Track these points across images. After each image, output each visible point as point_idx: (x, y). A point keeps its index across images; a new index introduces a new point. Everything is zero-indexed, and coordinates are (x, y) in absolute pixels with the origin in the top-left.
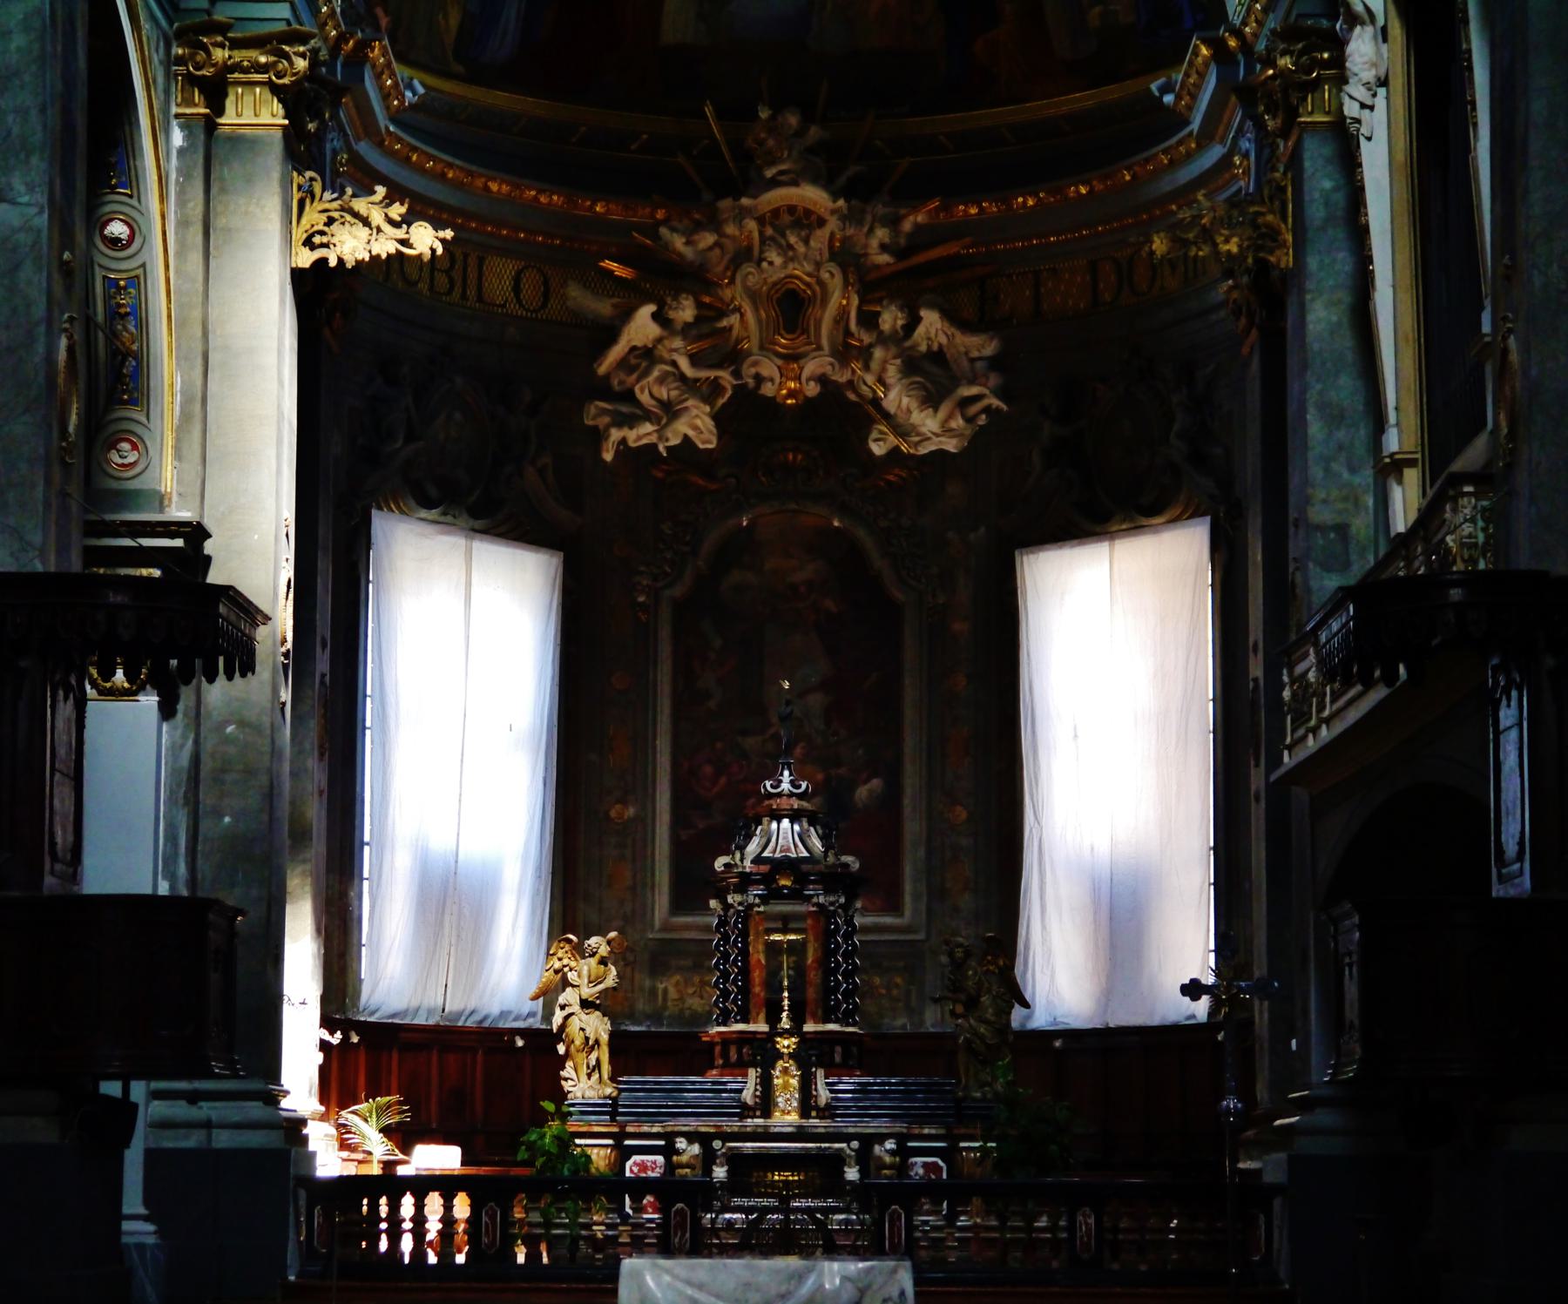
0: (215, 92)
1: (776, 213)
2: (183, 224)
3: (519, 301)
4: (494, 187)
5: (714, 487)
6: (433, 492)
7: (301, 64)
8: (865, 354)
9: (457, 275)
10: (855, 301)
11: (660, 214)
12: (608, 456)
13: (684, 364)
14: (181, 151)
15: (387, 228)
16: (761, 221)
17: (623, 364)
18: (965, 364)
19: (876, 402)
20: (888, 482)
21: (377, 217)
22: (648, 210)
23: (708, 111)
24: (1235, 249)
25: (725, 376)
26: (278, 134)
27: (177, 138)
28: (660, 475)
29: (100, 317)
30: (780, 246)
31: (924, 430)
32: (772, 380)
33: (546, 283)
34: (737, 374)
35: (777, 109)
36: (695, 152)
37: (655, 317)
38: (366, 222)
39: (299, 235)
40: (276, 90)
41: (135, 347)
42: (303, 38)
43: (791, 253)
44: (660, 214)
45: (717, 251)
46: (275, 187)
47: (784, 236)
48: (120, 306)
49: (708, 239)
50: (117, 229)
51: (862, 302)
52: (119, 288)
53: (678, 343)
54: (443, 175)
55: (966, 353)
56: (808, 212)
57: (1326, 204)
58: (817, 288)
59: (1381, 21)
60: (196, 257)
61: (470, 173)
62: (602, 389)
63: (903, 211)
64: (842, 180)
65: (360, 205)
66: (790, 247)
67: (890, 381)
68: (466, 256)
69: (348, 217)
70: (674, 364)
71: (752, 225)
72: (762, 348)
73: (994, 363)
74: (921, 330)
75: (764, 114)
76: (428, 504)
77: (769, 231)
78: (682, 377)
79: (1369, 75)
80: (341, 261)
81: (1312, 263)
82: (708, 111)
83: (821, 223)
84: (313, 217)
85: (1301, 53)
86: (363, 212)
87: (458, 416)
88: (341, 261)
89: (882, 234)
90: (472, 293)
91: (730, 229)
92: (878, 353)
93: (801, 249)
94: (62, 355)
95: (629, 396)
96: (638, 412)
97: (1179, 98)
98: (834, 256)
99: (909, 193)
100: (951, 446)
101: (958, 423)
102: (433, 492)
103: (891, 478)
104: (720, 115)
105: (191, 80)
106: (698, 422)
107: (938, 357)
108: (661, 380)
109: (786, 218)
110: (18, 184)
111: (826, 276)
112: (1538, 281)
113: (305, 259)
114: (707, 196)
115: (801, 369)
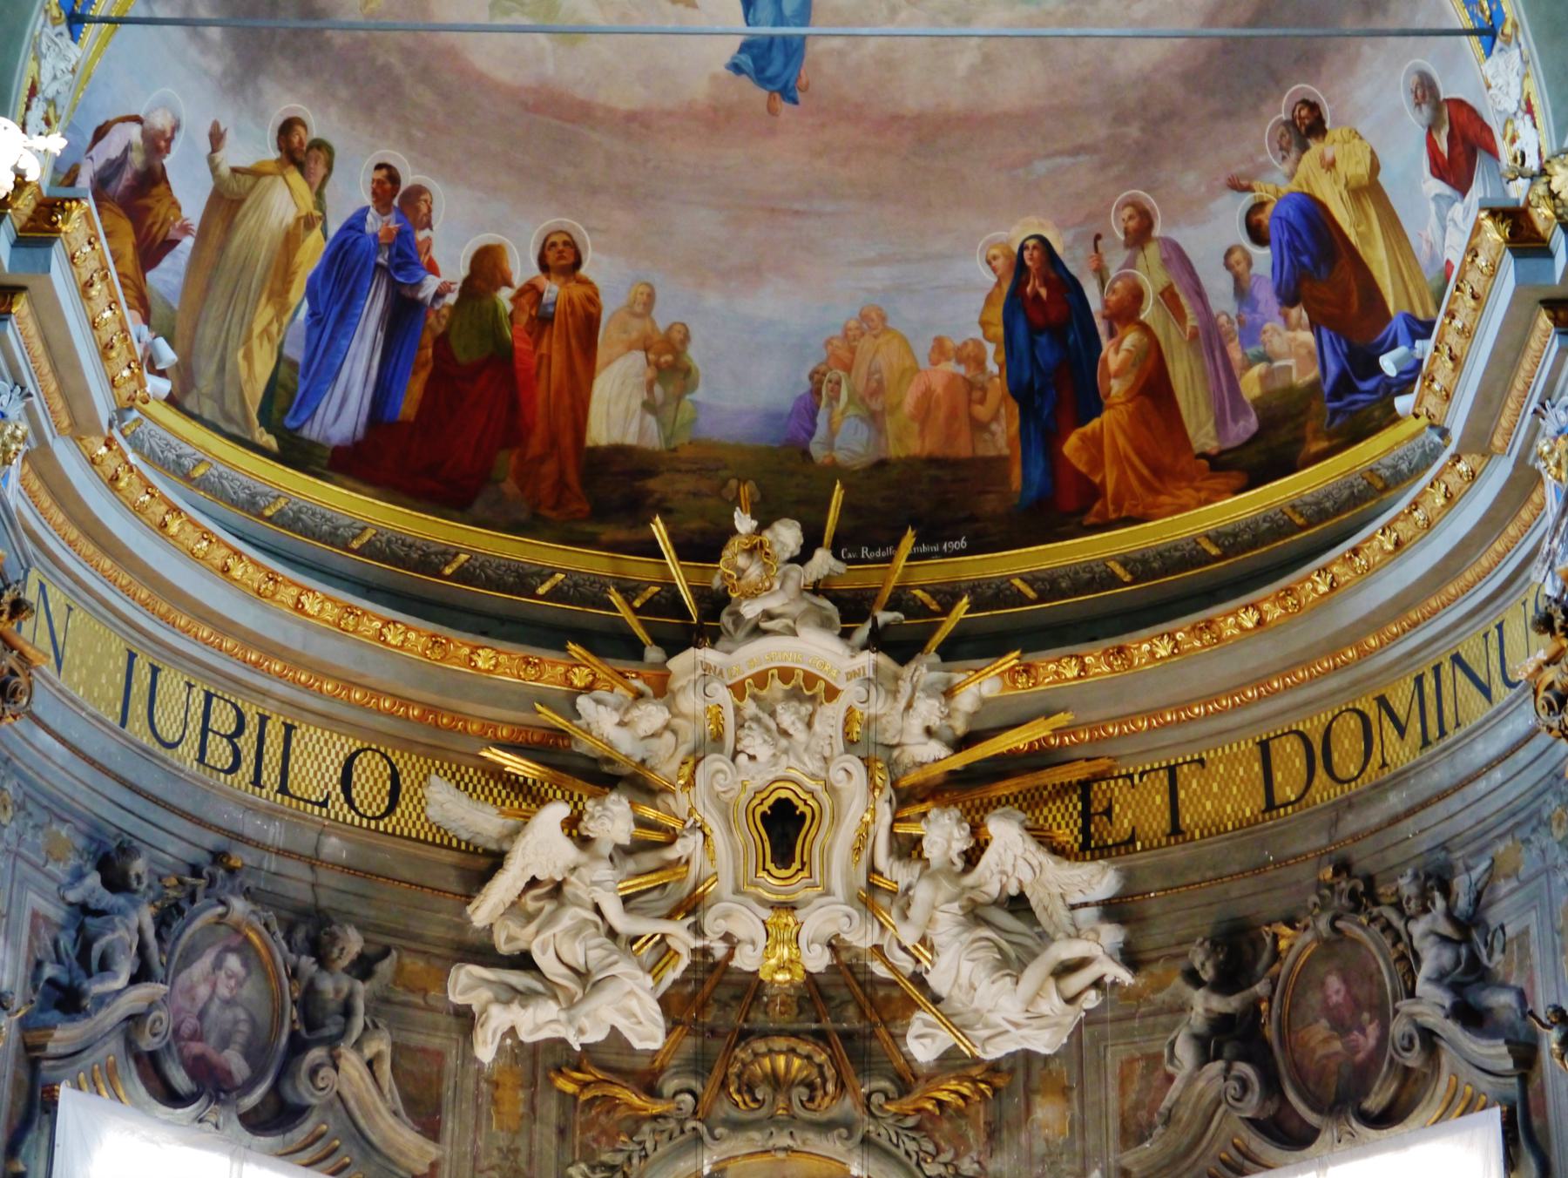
1: (761, 679)
3: (349, 800)
4: (311, 605)
5: (658, 1108)
6: (181, 1080)
8: (903, 899)
9: (247, 743)
10: (885, 815)
12: (485, 1052)
13: (613, 909)
16: (738, 690)
17: (514, 908)
18: (1063, 915)
19: (919, 980)
20: (940, 1104)
22: (561, 669)
23: (659, 529)
25: (679, 934)
28: (570, 1088)
30: (768, 730)
31: (996, 1018)
32: (753, 943)
33: (395, 777)
34: (697, 930)
36: (637, 604)
37: (571, 825)
43: (784, 742)
44: (580, 677)
45: (668, 736)
47: (773, 714)
49: (652, 715)
51: (896, 820)
53: (603, 871)
54: (225, 570)
55: (1062, 896)
56: (810, 679)
58: (824, 797)
61: (272, 577)
62: (483, 953)
63: (958, 678)
66: (785, 733)
67: (937, 940)
68: (263, 720)
70: (597, 909)
71: (724, 697)
72: (737, 891)
73: (1112, 910)
74: (988, 859)
75: (744, 523)
76: (173, 1098)
77: (750, 708)
78: (612, 934)
82: (659, 529)
83: (832, 693)
87: (233, 962)
89: (928, 710)
90: (271, 776)
91: (690, 702)
92: (922, 893)
93: (799, 733)
95: (524, 961)
96: (539, 987)
98: (850, 744)
100: (1044, 1042)
101: (1052, 1004)
102: (181, 1080)
103: (944, 1096)
106: (633, 1004)
107: (1018, 904)
108: (576, 931)
109: (777, 687)
111: (837, 776)
114: (653, 654)
115: (799, 924)
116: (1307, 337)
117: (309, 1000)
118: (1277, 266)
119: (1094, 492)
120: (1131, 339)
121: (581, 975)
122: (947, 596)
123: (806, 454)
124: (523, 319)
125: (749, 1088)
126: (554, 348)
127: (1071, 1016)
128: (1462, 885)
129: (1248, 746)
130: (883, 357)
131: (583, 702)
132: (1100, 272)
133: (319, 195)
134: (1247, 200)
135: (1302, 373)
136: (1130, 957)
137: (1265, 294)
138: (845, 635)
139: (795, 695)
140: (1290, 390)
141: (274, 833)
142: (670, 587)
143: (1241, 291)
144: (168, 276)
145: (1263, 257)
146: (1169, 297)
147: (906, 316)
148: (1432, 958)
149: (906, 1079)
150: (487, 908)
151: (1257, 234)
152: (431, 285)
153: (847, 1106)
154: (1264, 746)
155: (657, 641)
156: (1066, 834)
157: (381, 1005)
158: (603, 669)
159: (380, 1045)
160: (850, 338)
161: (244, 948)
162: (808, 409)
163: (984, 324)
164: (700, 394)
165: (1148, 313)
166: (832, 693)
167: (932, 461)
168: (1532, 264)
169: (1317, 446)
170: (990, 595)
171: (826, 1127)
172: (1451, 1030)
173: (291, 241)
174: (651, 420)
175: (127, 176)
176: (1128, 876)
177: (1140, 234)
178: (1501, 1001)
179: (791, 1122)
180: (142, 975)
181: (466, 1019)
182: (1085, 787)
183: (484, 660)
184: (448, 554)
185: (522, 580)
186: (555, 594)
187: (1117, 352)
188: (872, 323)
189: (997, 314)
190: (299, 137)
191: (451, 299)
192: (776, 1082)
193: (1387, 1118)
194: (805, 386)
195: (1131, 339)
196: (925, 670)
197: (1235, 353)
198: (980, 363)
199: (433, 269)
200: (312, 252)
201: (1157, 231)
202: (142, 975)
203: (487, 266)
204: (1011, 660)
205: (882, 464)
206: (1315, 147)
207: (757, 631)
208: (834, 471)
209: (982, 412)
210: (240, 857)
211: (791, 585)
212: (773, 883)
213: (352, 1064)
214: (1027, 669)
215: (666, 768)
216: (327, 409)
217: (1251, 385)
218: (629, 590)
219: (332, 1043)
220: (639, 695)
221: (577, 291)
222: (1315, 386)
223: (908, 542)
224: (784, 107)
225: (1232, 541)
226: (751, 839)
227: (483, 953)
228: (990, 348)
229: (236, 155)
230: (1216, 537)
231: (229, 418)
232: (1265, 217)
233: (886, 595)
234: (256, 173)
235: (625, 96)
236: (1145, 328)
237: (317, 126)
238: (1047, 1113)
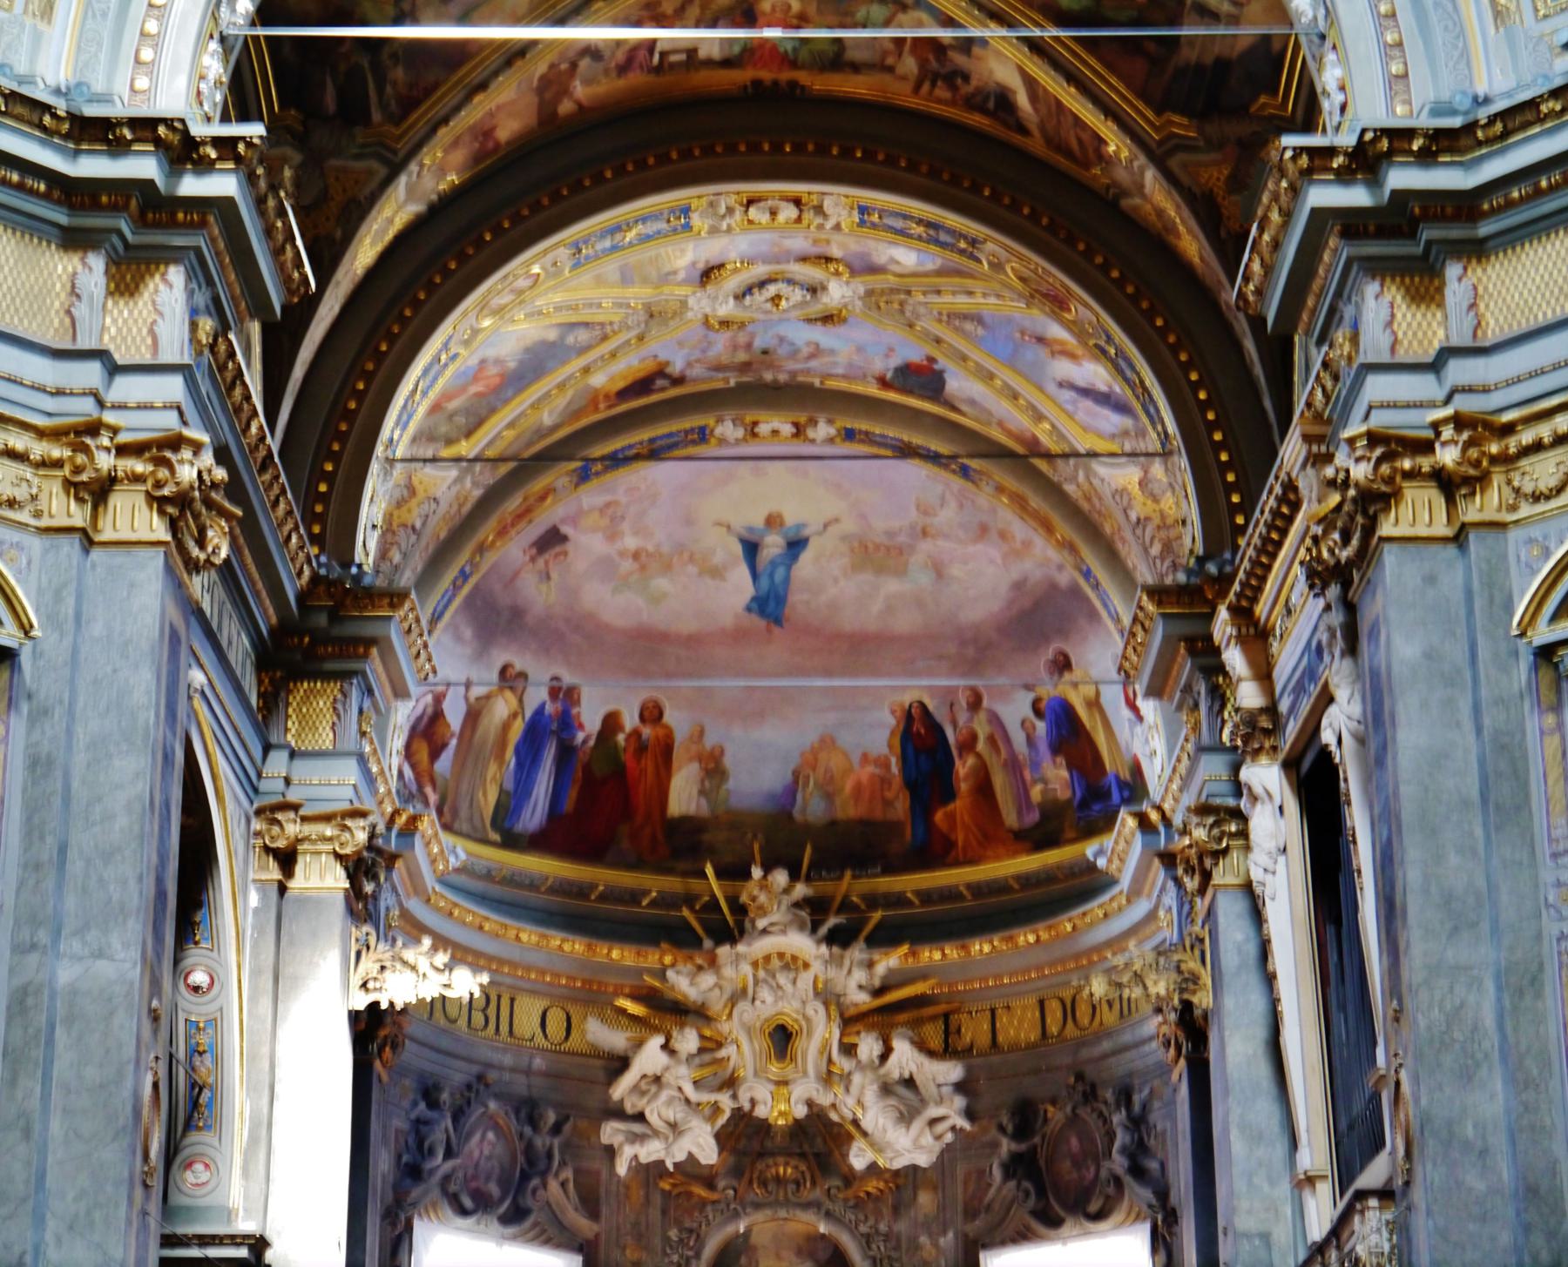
0: (287, 859)
1: (767, 958)
2: (256, 973)
3: (546, 1036)
4: (524, 937)
5: (714, 1196)
6: (468, 1202)
7: (362, 837)
8: (846, 1079)
9: (492, 1011)
10: (836, 1033)
11: (668, 959)
12: (622, 1169)
13: (689, 1089)
14: (256, 911)
15: (431, 973)
16: (755, 965)
17: (636, 1089)
18: (934, 1090)
19: (856, 1122)
20: (868, 1194)
21: (423, 964)
22: (657, 957)
23: (709, 870)
24: (1163, 992)
25: (725, 1101)
26: (341, 895)
27: (254, 899)
28: (667, 1187)
29: (181, 1054)
30: (771, 987)
31: (898, 1147)
32: (765, 1104)
33: (568, 1014)
34: (735, 1097)
35: (767, 869)
36: (697, 907)
37: (666, 1047)
38: (414, 968)
39: (356, 981)
40: (338, 856)
41: (211, 1080)
42: (363, 814)
43: (780, 993)
45: (717, 991)
46: (337, 939)
47: (774, 977)
48: (198, 1044)
49: (707, 980)
50: (199, 978)
51: (842, 1035)
52: (198, 1029)
53: (683, 1070)
55: (934, 1080)
56: (794, 958)
57: (1240, 951)
58: (804, 1023)
59: (1277, 802)
60: (266, 1003)
62: (618, 1113)
63: (876, 957)
64: (823, 930)
65: (409, 955)
66: (779, 987)
67: (866, 1104)
68: (499, 997)
69: (398, 966)
70: (680, 1089)
71: (746, 969)
72: (756, 1074)
73: (960, 1087)
74: (893, 1059)
75: (757, 872)
76: (463, 1212)
77: (761, 974)
78: (688, 1101)
79: (1271, 845)
80: (392, 1004)
81: (1229, 1002)
82: (709, 870)
83: (806, 966)
84: (368, 965)
85: (1212, 826)
86: (411, 960)
87: (491, 1135)
88: (392, 1004)
89: (859, 976)
90: (504, 1028)
91: (728, 972)
92: (857, 1079)
93: (789, 988)
94: (147, 1090)
95: (640, 1117)
96: (649, 1132)
97: (1110, 861)
98: (817, 994)
99: (884, 938)
100: (923, 1160)
101: (927, 1139)
102: (468, 1202)
103: (870, 1189)
104: (719, 875)
105: (267, 850)
106: (701, 1140)
107: (910, 1083)
108: (670, 1102)
109: (776, 963)
110: (116, 942)
111: (810, 1012)
112: (1422, 1022)
113: (361, 1002)
114: (708, 944)
115: (790, 1094)
116: (1065, 773)
117: (529, 1149)
118: (1049, 732)
119: (949, 844)
120: (971, 761)
121: (673, 1126)
122: (873, 901)
123: (790, 816)
124: (631, 749)
125: (764, 1184)
126: (649, 764)
127: (937, 1147)
128: (1137, 1099)
129: (1032, 1001)
130: (835, 762)
131: (670, 974)
132: (954, 723)
133: (521, 701)
134: (1031, 696)
135: (1063, 794)
136: (970, 1114)
137: (1043, 747)
138: (814, 930)
139: (786, 967)
140: (1056, 801)
141: (508, 1060)
142: (713, 896)
143: (1030, 741)
144: (444, 764)
145: (1041, 727)
146: (991, 740)
147: (846, 739)
148: (1121, 1138)
149: (850, 1178)
150: (620, 1089)
151: (1038, 712)
152: (580, 736)
153: (817, 1194)
154: (1042, 1003)
155: (710, 932)
156: (936, 1042)
157: (565, 1147)
158: (681, 954)
159: (568, 1173)
160: (815, 752)
161: (497, 1127)
162: (791, 791)
163: (890, 746)
164: (731, 784)
165: (981, 746)
166: (806, 966)
167: (865, 824)
168: (1149, 838)
169: (1070, 834)
170: (899, 900)
171: (807, 1206)
172: (1128, 1180)
173: (506, 727)
174: (703, 802)
175: (426, 719)
176: (969, 1070)
177: (975, 703)
178: (1153, 1165)
179: (787, 1203)
180: (449, 1154)
181: (611, 1152)
182: (946, 1016)
183: (615, 954)
184: (593, 886)
185: (634, 897)
186: (653, 904)
187: (963, 768)
188: (827, 742)
189: (897, 742)
190: (510, 672)
191: (592, 743)
192: (778, 1180)
193: (1099, 1216)
194: (789, 777)
195: (971, 761)
196: (857, 952)
197: (1027, 775)
198: (887, 766)
199: (581, 726)
200: (517, 729)
201: (985, 703)
202: (449, 1154)
203: (611, 723)
204: (905, 949)
205: (833, 823)
206: (1067, 676)
207: (765, 932)
208: (807, 830)
209: (889, 795)
210: (492, 1076)
211: (783, 907)
212: (774, 1069)
213: (554, 1185)
214: (914, 954)
215: (717, 1005)
216: (526, 814)
217: (1036, 793)
218: (689, 900)
219: (544, 1174)
220: (700, 968)
221: (661, 732)
222: (1069, 802)
223: (848, 874)
224: (776, 630)
225: (1027, 881)
226: (762, 1044)
227: (618, 1113)
228: (893, 760)
229: (477, 691)
230: (1018, 878)
231: (474, 828)
232: (1043, 705)
233: (839, 899)
234: (488, 697)
235: (688, 626)
236: (979, 756)
237: (519, 664)
238: (925, 1199)
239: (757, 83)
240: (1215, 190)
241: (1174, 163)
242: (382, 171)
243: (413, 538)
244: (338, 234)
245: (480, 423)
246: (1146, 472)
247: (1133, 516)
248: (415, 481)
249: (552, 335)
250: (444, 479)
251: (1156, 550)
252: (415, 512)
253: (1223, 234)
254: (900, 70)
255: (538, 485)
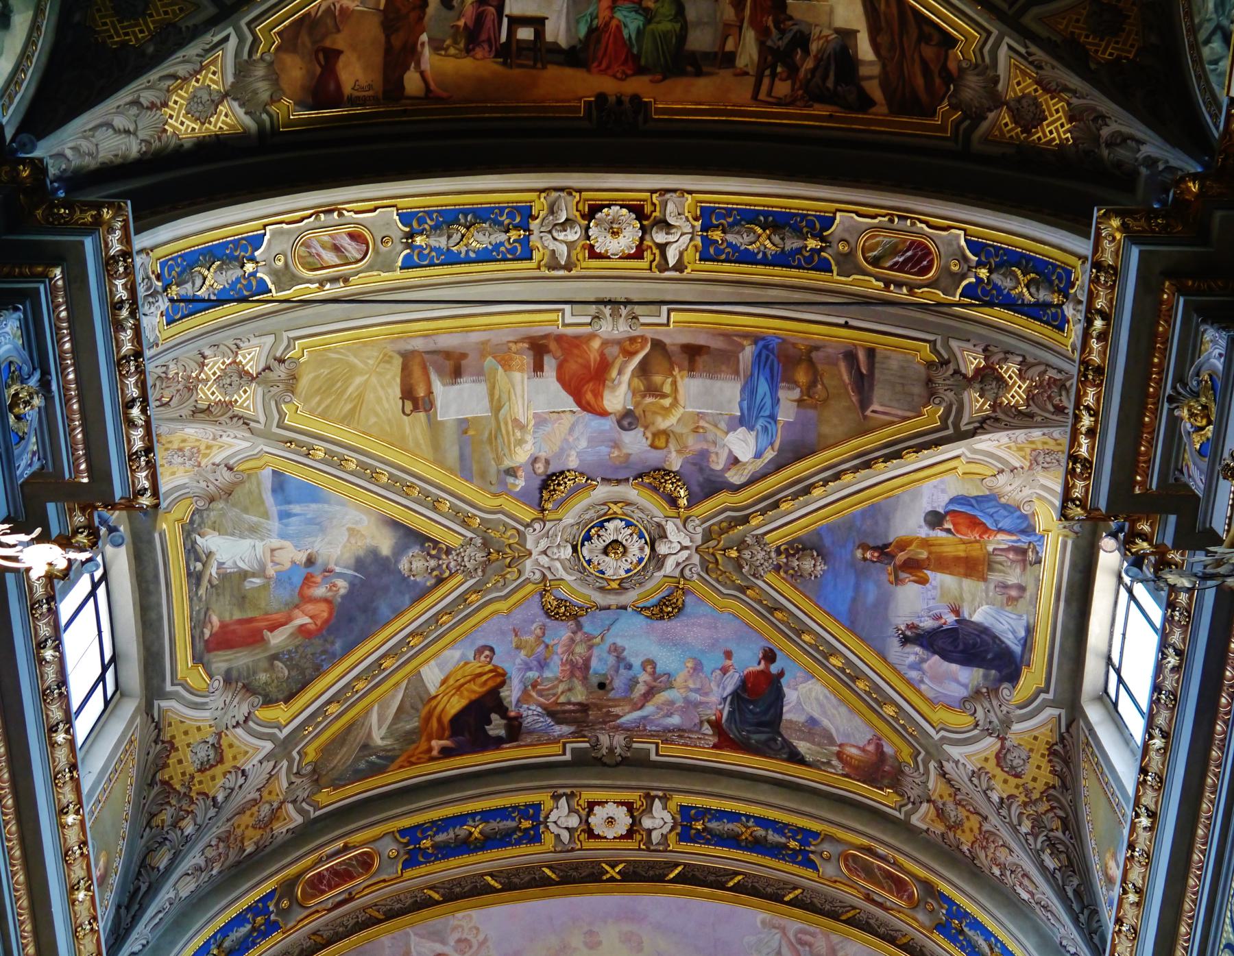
239: (601, 97)
240: (1077, 31)
241: (1028, 20)
242: (211, 10)
243: (212, 812)
244: (151, 49)
245: (304, 686)
246: (1003, 739)
247: (995, 797)
248: (224, 743)
249: (385, 544)
250: (257, 749)
251: (1026, 827)
252: (220, 781)
253: (1093, 66)
254: (741, 62)
255: (361, 837)
